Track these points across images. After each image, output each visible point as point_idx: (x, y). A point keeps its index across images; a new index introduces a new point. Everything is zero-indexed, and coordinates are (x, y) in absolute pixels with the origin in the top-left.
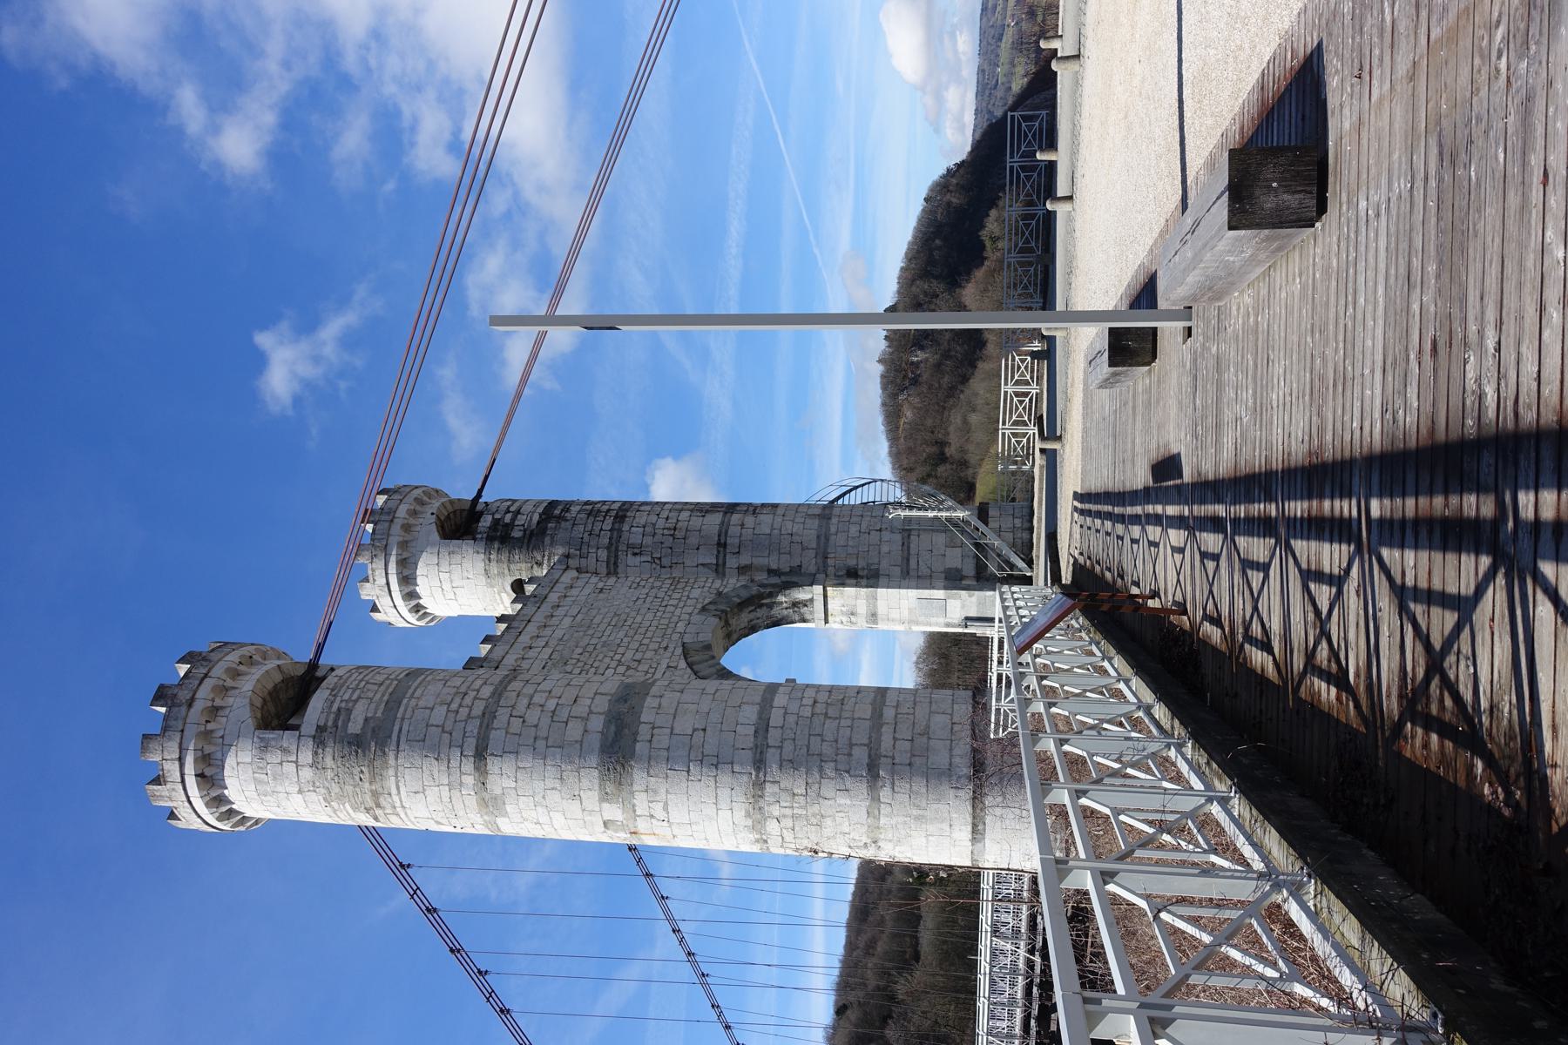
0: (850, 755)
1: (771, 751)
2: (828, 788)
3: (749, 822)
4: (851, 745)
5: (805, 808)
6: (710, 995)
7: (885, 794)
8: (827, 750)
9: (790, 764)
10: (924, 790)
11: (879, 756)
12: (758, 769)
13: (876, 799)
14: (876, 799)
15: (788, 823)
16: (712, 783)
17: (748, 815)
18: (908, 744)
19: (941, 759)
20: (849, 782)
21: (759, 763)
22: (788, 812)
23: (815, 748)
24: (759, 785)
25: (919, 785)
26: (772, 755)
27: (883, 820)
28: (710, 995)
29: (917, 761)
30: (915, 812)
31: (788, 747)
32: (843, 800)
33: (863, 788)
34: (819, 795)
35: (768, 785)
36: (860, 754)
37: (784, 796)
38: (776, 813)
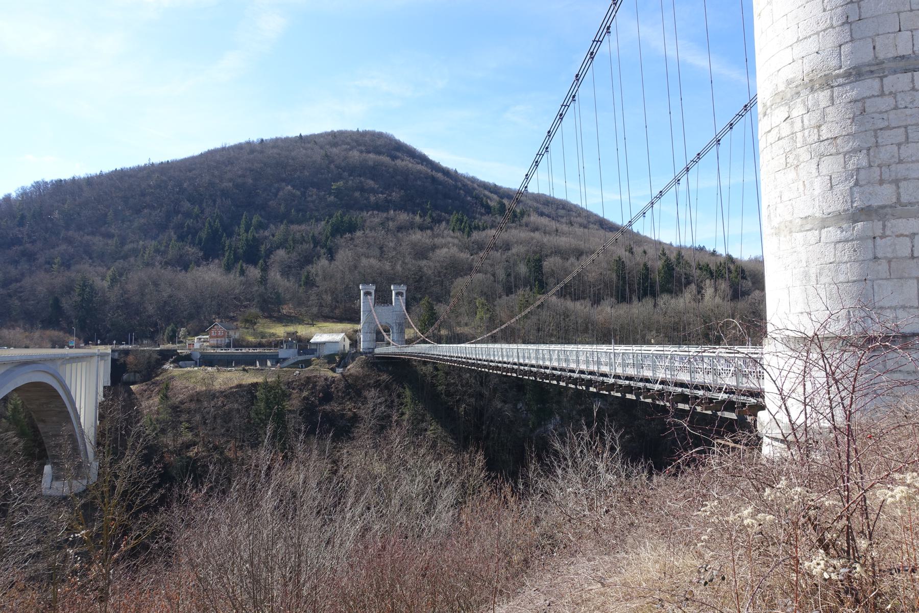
0: (881, 182)
1: (876, 83)
2: (832, 165)
3: (782, 87)
4: (896, 182)
5: (805, 144)
6: (706, 149)
7: (832, 233)
8: (886, 153)
9: (860, 111)
10: (842, 278)
11: (883, 218)
12: (847, 74)
13: (824, 224)
14: (824, 224)
15: (786, 130)
16: (822, 27)
17: (789, 82)
18: (907, 252)
19: (887, 294)
20: (842, 188)
21: (856, 74)
22: (798, 126)
23: (884, 137)
24: (827, 83)
25: (848, 272)
26: (871, 85)
27: (799, 236)
28: (706, 149)
29: (883, 266)
30: (813, 271)
31: (886, 103)
32: (819, 186)
33: (837, 205)
34: (822, 155)
35: (827, 93)
36: (885, 195)
37: (815, 117)
38: (795, 113)
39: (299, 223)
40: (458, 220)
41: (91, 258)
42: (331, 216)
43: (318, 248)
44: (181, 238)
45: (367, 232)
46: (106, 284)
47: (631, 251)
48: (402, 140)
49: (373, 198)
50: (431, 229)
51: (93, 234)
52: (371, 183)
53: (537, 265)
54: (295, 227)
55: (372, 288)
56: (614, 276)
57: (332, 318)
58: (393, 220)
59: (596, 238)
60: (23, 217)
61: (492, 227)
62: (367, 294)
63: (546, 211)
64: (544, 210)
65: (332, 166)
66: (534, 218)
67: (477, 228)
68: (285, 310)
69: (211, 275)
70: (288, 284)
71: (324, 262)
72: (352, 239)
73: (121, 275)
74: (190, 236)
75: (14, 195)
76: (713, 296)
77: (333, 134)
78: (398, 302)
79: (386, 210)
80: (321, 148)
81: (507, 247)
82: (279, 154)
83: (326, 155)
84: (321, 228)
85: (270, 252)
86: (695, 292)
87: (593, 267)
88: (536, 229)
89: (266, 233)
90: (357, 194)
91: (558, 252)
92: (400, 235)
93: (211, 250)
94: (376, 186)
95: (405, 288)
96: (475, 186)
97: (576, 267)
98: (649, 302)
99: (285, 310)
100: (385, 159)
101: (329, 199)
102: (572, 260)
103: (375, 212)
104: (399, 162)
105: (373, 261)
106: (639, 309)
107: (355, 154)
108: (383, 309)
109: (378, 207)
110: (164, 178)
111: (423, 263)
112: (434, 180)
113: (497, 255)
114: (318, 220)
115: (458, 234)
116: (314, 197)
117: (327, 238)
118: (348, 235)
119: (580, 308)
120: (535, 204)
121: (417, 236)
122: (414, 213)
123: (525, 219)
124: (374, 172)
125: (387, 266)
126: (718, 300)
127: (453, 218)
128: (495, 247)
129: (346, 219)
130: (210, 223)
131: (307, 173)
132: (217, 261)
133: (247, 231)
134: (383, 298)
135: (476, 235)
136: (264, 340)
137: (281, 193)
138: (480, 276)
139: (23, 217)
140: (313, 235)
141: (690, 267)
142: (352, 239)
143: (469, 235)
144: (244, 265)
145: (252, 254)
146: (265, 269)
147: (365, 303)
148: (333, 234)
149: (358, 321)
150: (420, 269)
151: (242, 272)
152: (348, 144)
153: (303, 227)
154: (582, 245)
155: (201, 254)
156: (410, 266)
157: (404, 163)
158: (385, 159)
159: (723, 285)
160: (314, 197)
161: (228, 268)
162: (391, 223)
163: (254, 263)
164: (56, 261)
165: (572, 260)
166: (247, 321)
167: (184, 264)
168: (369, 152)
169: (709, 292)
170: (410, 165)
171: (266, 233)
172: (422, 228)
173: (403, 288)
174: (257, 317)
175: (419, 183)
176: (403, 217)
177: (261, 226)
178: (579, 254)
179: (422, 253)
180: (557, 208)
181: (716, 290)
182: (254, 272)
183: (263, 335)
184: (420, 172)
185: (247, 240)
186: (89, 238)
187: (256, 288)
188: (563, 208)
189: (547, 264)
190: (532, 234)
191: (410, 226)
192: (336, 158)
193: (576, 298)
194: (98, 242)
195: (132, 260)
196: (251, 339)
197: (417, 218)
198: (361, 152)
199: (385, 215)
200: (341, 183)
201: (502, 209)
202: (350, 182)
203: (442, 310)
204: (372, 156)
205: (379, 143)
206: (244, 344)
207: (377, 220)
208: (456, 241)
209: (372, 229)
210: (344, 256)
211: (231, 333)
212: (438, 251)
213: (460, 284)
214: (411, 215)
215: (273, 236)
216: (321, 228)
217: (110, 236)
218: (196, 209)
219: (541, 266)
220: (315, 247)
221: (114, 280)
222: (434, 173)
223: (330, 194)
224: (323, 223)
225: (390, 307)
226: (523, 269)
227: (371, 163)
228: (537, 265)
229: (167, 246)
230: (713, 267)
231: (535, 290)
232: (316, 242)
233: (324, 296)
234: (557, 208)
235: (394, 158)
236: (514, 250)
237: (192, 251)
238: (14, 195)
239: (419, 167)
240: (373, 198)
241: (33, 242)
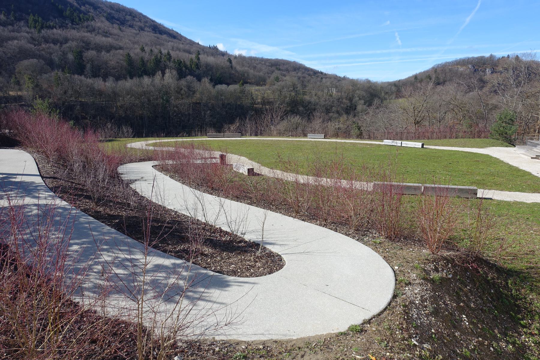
50: (12, 25)
63: (116, 16)
64: (115, 16)
88: (92, 30)
98: (136, 80)
120: (109, 11)
123: (86, 24)
126: (171, 80)
127: (31, 18)
128: (55, 42)
143: (39, 32)
165: (103, 53)
180: (126, 15)
188: (130, 15)
212: (10, 42)
226: (70, 56)
228: (79, 55)
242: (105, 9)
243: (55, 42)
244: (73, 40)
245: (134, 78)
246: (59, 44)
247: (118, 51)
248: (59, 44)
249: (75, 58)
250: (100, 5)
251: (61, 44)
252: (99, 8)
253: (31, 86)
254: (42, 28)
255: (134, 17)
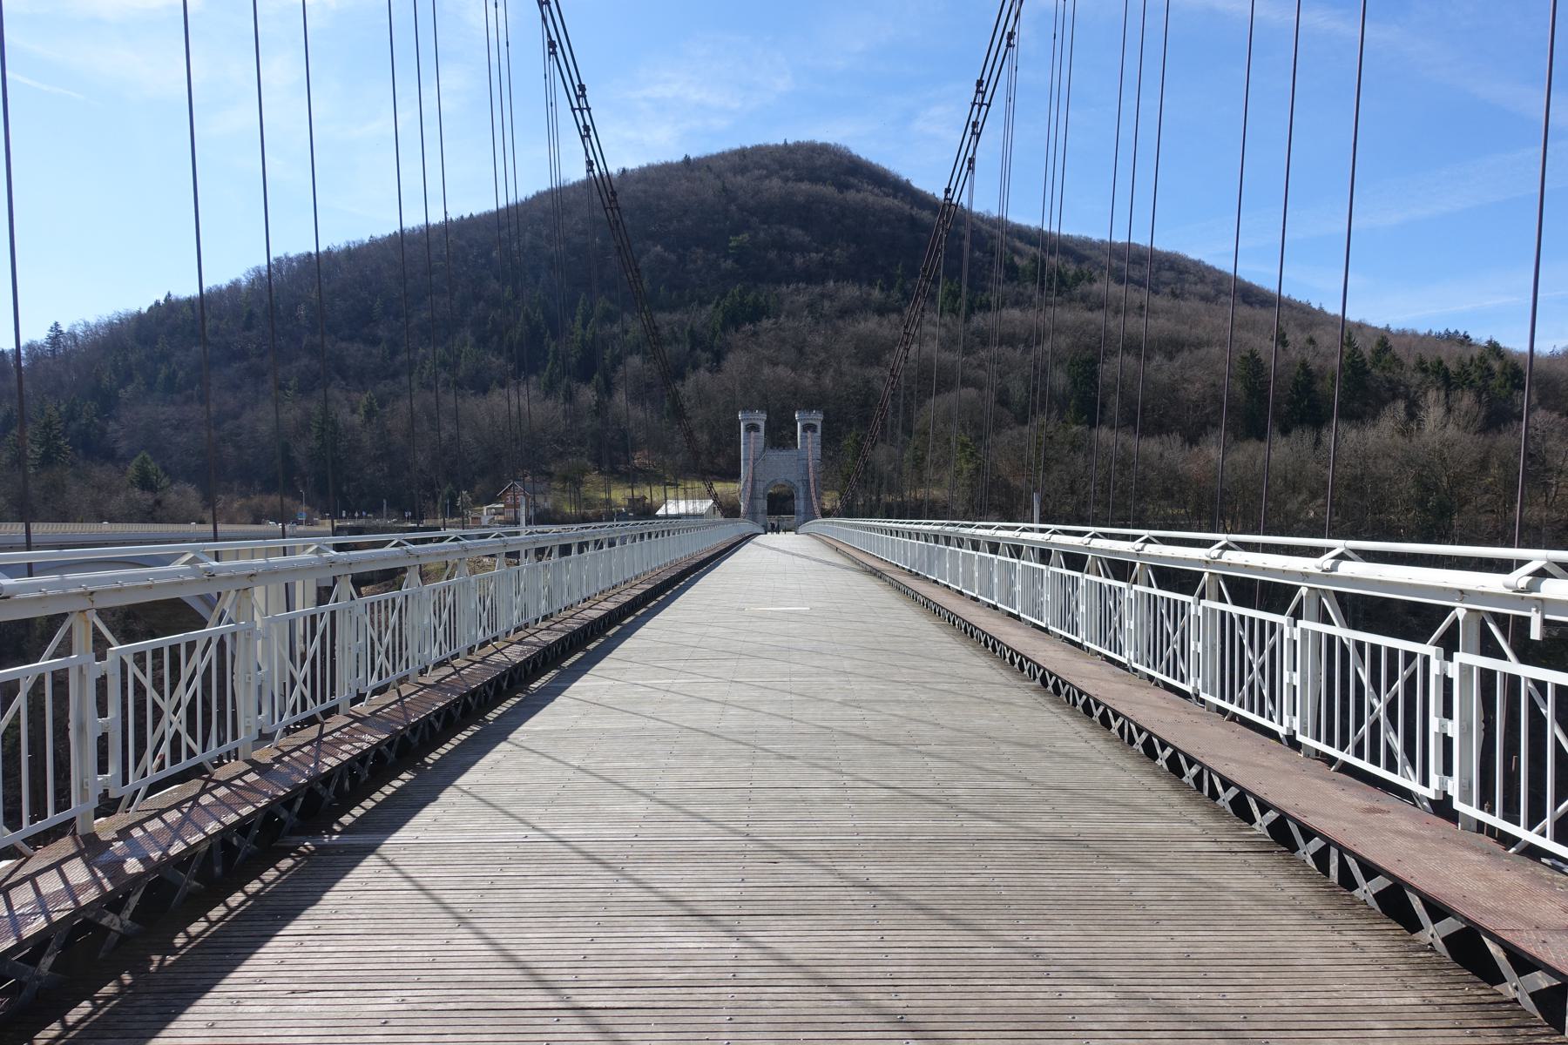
39: (673, 308)
40: (950, 293)
41: (344, 378)
42: (724, 296)
43: (699, 351)
44: (482, 341)
45: (782, 319)
46: (357, 419)
47: (1282, 340)
48: (863, 157)
49: (799, 261)
50: (900, 311)
51: (351, 339)
52: (797, 234)
53: (1086, 369)
54: (662, 317)
55: (760, 418)
56: (1239, 387)
57: (712, 473)
58: (831, 298)
59: (1215, 320)
60: (251, 315)
61: (1017, 303)
62: (752, 428)
65: (733, 207)
66: (1104, 287)
67: (986, 307)
68: (639, 459)
69: (521, 404)
70: (641, 415)
71: (703, 374)
72: (755, 334)
73: (382, 405)
74: (495, 338)
75: (244, 283)
76: (1440, 426)
77: (742, 153)
78: (808, 444)
79: (822, 280)
80: (718, 177)
81: (1032, 338)
82: (645, 192)
83: (725, 189)
84: (704, 316)
85: (618, 360)
86: (1402, 415)
87: (1205, 374)
88: (1101, 306)
89: (616, 329)
90: (772, 255)
91: (1132, 345)
92: (840, 323)
93: (526, 362)
94: (807, 239)
95: (820, 417)
96: (997, 232)
97: (1162, 369)
98: (1302, 439)
99: (639, 459)
100: (829, 191)
101: (723, 265)
102: (1158, 358)
103: (802, 285)
104: (851, 195)
105: (783, 372)
106: (1281, 451)
107: (776, 182)
108: (778, 457)
109: (809, 277)
110: (463, 243)
111: (874, 372)
112: (913, 222)
113: (1016, 354)
114: (703, 303)
115: (947, 318)
116: (700, 263)
117: (715, 333)
118: (748, 327)
119: (1163, 451)
120: (1115, 263)
121: (869, 325)
122: (871, 284)
124: (805, 214)
125: (807, 380)
126: (1451, 431)
128: (1009, 340)
129: (750, 298)
130: (527, 316)
131: (689, 223)
132: (534, 378)
133: (584, 326)
134: (779, 435)
135: (978, 320)
136: (590, 512)
137: (644, 259)
138: (972, 392)
139: (251, 315)
140: (691, 331)
141: (1402, 366)
142: (755, 334)
143: (967, 319)
144: (574, 385)
145: (591, 365)
146: (608, 389)
147: (750, 445)
148: (724, 328)
149: (734, 475)
150: (867, 381)
151: (569, 397)
152: (766, 167)
153: (676, 316)
154: (1184, 331)
155: (510, 367)
156: (848, 378)
157: (861, 195)
158: (829, 191)
159: (1466, 400)
160: (700, 263)
161: (550, 389)
162: (827, 304)
163: (586, 378)
164: (291, 383)
165: (1158, 358)
166: (565, 479)
167: (481, 385)
168: (801, 180)
169: (1433, 414)
170: (871, 199)
171: (616, 329)
172: (882, 311)
173: (817, 418)
174: (584, 472)
175: (885, 229)
176: (851, 291)
177: (609, 317)
178: (1173, 347)
179: (872, 353)
180: (1159, 269)
181: (1449, 410)
182: (588, 395)
183: (589, 503)
184: (888, 210)
185: (583, 340)
186: (344, 345)
187: (587, 422)
188: (1171, 268)
189: (1110, 369)
190: (1088, 315)
191: (864, 306)
192: (740, 193)
193: (1156, 426)
194: (355, 352)
195: (404, 379)
196: (569, 509)
197: (876, 293)
198: (786, 180)
199: (818, 290)
200: (745, 237)
201: (1039, 274)
202: (762, 234)
203: (881, 455)
204: (805, 186)
205: (819, 163)
206: (558, 517)
207: (802, 299)
208: (943, 332)
209: (791, 314)
210: (736, 362)
211: (540, 500)
213: (935, 405)
214: (865, 288)
215: (626, 332)
216: (704, 316)
217: (375, 342)
218: (508, 292)
219: (1094, 373)
220: (693, 348)
221: (370, 413)
222: (915, 211)
223: (726, 257)
224: (711, 307)
225: (793, 452)
226: (1060, 379)
227: (801, 199)
228: (1086, 369)
229: (459, 356)
230: (1453, 367)
231: (1070, 415)
232: (697, 341)
233: (697, 435)
234: (1159, 269)
235: (843, 187)
236: (1048, 345)
237: (496, 362)
238: (244, 283)
239: (889, 202)
240: (799, 261)
241: (261, 356)
242: (1105, 259)
243: (1009, 340)
244: (1057, 330)
245: (1295, 434)
246: (1021, 346)
247: (1202, 352)
248: (1021, 346)
249: (1075, 382)
250: (1088, 252)
251: (1028, 347)
252: (1087, 258)
253: (967, 467)
254: (971, 310)
255: (1181, 273)
